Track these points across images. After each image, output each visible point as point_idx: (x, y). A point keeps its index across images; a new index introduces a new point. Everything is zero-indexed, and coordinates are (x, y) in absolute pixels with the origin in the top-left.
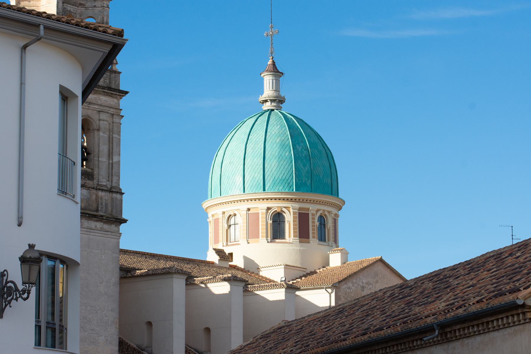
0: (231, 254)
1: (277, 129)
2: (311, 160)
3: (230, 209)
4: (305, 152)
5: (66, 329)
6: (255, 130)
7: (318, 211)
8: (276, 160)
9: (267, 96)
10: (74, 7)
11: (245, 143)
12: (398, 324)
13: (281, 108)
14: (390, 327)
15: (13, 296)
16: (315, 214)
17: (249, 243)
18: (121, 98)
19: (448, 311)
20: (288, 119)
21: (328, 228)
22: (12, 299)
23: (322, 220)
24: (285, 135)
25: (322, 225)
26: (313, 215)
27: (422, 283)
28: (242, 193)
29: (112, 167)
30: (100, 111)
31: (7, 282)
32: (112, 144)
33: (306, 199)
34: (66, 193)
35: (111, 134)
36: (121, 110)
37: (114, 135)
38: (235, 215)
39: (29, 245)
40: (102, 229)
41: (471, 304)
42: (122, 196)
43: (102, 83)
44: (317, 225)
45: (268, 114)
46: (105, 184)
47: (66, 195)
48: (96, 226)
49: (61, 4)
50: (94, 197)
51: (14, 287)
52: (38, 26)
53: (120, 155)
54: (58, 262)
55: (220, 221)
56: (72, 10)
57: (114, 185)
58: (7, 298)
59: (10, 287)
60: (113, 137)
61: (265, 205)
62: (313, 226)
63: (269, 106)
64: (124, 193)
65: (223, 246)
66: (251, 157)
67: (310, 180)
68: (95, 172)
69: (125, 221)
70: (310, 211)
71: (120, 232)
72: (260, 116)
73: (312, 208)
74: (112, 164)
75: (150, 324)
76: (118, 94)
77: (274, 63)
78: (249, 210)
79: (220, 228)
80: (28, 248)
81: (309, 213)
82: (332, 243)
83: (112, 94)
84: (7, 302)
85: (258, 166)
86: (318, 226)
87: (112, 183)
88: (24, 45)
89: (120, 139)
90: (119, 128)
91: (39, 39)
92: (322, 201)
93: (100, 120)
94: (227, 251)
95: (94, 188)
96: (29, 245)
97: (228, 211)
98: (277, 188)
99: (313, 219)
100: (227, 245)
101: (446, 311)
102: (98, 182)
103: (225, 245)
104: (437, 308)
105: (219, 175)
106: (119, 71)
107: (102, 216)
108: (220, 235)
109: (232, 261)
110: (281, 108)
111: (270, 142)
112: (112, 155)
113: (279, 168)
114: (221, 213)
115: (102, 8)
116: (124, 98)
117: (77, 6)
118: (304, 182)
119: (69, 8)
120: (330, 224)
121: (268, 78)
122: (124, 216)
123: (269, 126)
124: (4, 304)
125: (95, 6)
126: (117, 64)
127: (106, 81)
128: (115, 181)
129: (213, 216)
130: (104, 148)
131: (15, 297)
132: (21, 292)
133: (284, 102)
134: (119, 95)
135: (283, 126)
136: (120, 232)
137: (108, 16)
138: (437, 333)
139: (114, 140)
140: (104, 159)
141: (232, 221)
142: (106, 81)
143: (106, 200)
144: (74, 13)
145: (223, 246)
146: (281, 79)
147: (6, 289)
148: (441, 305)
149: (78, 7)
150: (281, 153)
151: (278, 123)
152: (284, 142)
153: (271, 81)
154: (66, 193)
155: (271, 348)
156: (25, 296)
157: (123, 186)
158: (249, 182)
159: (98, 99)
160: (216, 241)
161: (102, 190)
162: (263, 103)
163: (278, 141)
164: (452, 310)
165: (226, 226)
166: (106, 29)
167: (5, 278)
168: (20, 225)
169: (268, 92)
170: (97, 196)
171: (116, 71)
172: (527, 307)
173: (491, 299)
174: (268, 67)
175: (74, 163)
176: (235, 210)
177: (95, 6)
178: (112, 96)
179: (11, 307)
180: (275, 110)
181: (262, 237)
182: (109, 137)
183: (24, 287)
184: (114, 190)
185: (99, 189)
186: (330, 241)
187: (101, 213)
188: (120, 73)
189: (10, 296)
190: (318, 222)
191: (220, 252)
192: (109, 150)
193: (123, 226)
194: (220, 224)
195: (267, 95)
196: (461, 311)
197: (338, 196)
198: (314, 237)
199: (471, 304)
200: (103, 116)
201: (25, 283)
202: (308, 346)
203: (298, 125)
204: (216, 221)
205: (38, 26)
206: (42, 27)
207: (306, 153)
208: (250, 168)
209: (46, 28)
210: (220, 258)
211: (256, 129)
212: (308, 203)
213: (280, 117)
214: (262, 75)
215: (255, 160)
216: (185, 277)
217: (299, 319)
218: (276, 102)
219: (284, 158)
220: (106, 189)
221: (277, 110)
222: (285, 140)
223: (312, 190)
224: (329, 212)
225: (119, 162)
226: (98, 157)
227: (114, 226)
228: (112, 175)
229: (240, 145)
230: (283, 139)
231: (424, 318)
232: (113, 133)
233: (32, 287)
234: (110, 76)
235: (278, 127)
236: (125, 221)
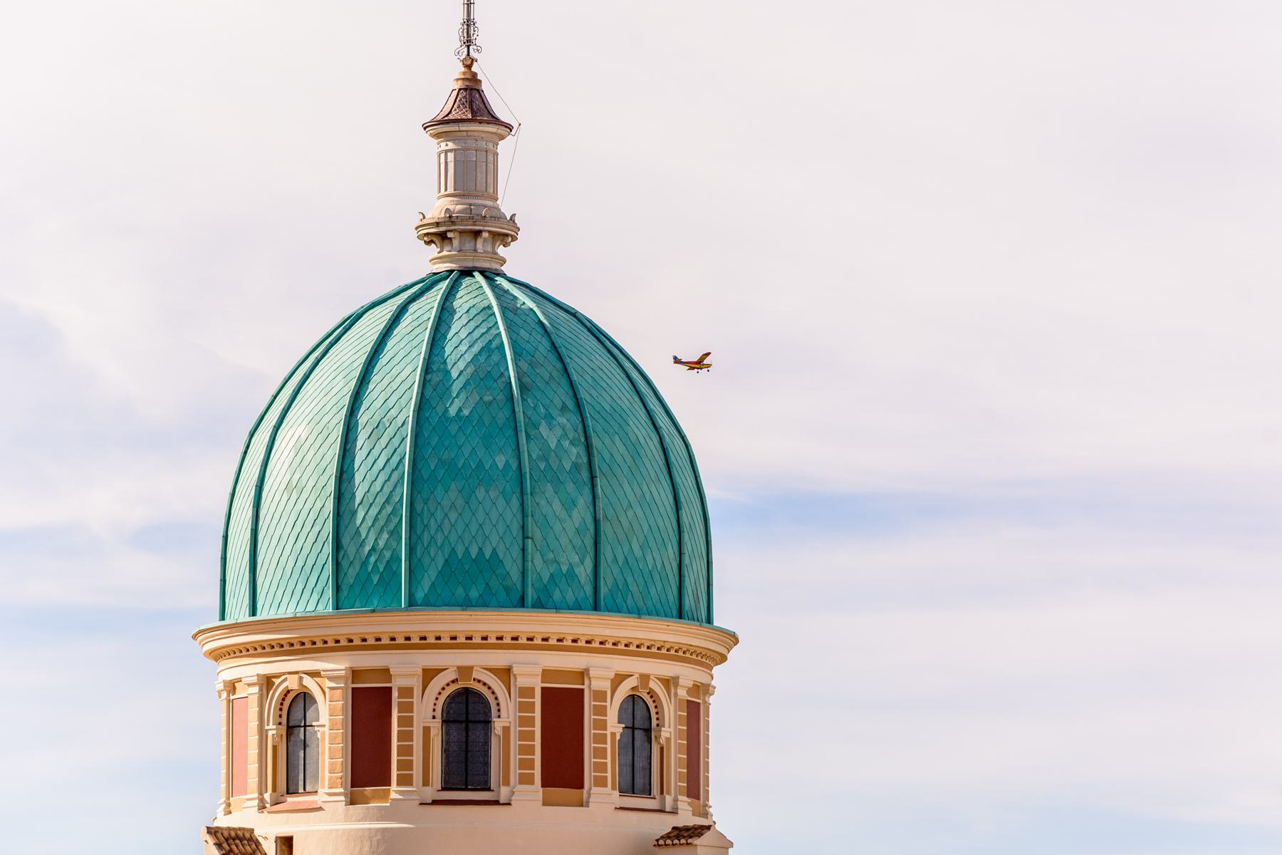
1: (468, 357)
4: (574, 450)
7: (619, 679)
16: (606, 692)
20: (515, 311)
23: (640, 713)
25: (638, 734)
26: (600, 695)
33: (570, 638)
44: (613, 734)
45: (442, 291)
67: (589, 563)
70: (586, 682)
73: (601, 669)
78: (356, 674)
81: (582, 690)
82: (676, 800)
86: (618, 737)
92: (637, 642)
99: (602, 711)
118: (564, 569)
120: (670, 730)
133: (514, 239)
145: (262, 807)
151: (477, 334)
186: (669, 793)
190: (619, 722)
195: (443, 215)
207: (578, 453)
212: (581, 650)
213: (489, 307)
224: (669, 683)
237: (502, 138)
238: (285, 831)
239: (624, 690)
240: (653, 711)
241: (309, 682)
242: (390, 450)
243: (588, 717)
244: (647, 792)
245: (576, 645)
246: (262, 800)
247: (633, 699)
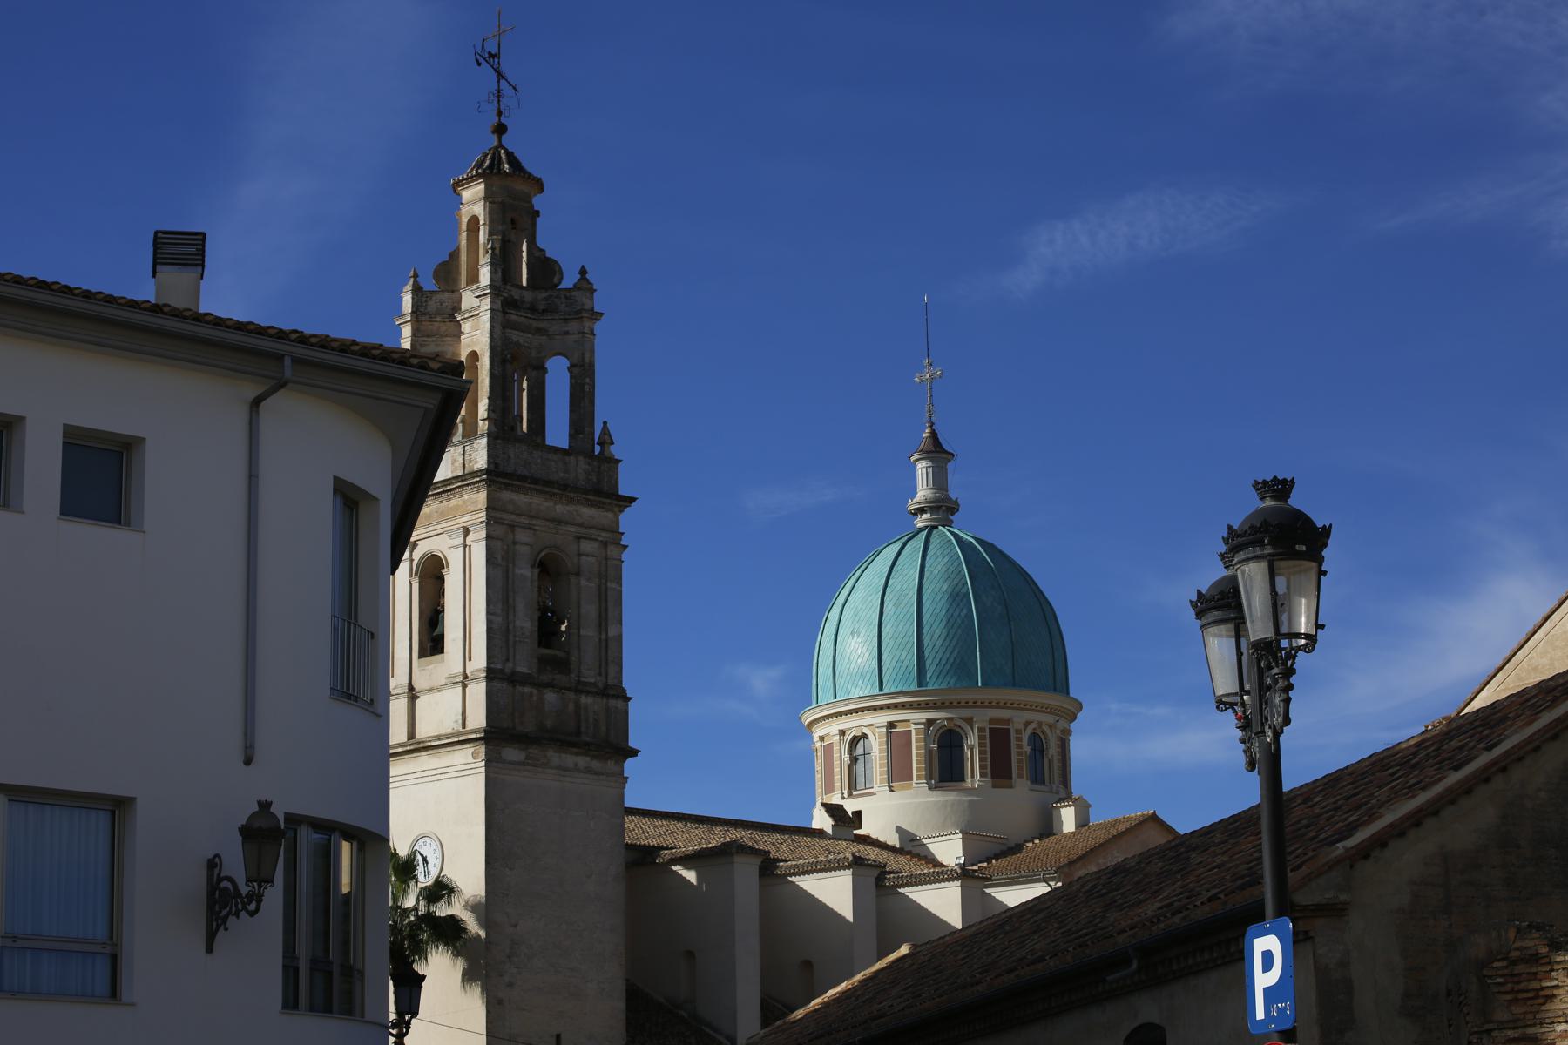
0: (858, 814)
1: (943, 563)
2: (1012, 623)
3: (853, 724)
5: (362, 973)
6: (899, 568)
7: (1027, 724)
8: (942, 626)
9: (922, 499)
10: (525, 335)
11: (880, 593)
12: (1071, 949)
13: (952, 522)
14: (1056, 955)
15: (231, 908)
17: (892, 791)
18: (621, 511)
19: (1159, 920)
21: (1050, 757)
22: (229, 913)
25: (1037, 753)
26: (1018, 731)
27: (1147, 864)
28: (877, 692)
29: (607, 647)
30: (579, 538)
31: (220, 879)
32: (606, 601)
34: (356, 699)
35: (604, 581)
36: (623, 534)
37: (609, 584)
38: (865, 736)
39: (259, 803)
40: (588, 770)
41: (1198, 903)
42: (627, 705)
43: (583, 483)
44: (1026, 752)
46: (593, 680)
47: (356, 701)
48: (576, 765)
49: (498, 329)
50: (571, 707)
51: (231, 888)
52: (281, 358)
53: (621, 624)
54: (337, 833)
55: (836, 748)
56: (521, 341)
57: (610, 682)
58: (220, 912)
59: (226, 889)
60: (606, 589)
61: (922, 716)
62: (1019, 754)
63: (927, 520)
64: (630, 698)
65: (843, 798)
66: (892, 620)
68: (573, 659)
69: (634, 753)
71: (625, 775)
72: (909, 539)
73: (1018, 719)
74: (607, 640)
75: (690, 955)
76: (616, 502)
77: (934, 434)
78: (891, 725)
79: (836, 763)
80: (257, 809)
82: (1058, 787)
83: (603, 503)
84: (219, 921)
85: (906, 639)
87: (606, 677)
88: (254, 400)
89: (620, 593)
90: (619, 569)
91: (281, 385)
93: (580, 555)
94: (850, 806)
95: (569, 689)
96: (259, 803)
97: (850, 729)
98: (948, 679)
99: (1019, 739)
100: (850, 795)
101: (1155, 920)
102: (579, 677)
103: (846, 795)
104: (1143, 915)
105: (831, 658)
106: (616, 457)
107: (587, 744)
108: (837, 777)
109: (860, 827)
110: (952, 522)
111: (930, 590)
112: (606, 625)
113: (948, 640)
114: (837, 732)
115: (581, 335)
116: (626, 510)
117: (529, 333)
119: (516, 336)
120: (1053, 750)
121: (924, 464)
122: (632, 743)
123: (928, 558)
124: (215, 924)
125: (567, 333)
126: (612, 443)
127: (590, 477)
128: (612, 670)
129: (822, 739)
130: (590, 610)
131: (234, 909)
132: (245, 900)
133: (958, 510)
134: (616, 505)
135: (954, 558)
136: (625, 775)
137: (592, 351)
138: (1135, 966)
139: (609, 593)
140: (589, 631)
141: (860, 750)
142: (590, 477)
143: (594, 712)
144: (525, 347)
145: (843, 798)
146: (950, 466)
147: (217, 892)
148: (1151, 908)
149: (533, 334)
150: (951, 611)
152: (956, 590)
153: (930, 470)
154: (356, 699)
155: (864, 1002)
156: (252, 907)
157: (628, 684)
158: (889, 672)
159: (575, 513)
160: (829, 789)
161: (588, 693)
162: (915, 514)
163: (945, 587)
164: (1165, 917)
165: (846, 758)
166: (426, 362)
167: (216, 871)
168: (248, 761)
169: (923, 491)
170: (577, 704)
171: (610, 458)
172: (1297, 908)
173: (1234, 892)
174: (923, 444)
175: (372, 634)
176: (865, 726)
177: (567, 333)
178: (603, 508)
179: (226, 929)
180: (940, 528)
181: (919, 778)
182: (599, 587)
183: (250, 888)
184: (611, 693)
185: (582, 692)
186: (1054, 783)
187: (585, 738)
188: (618, 461)
189: (225, 908)
191: (834, 811)
192: (600, 616)
193: (630, 765)
194: (836, 755)
196: (1177, 919)
197: (1068, 693)
198: (1021, 776)
199: (1198, 903)
200: (587, 546)
201: (251, 881)
202: (920, 996)
203: (985, 555)
204: (828, 749)
205: (281, 358)
206: (287, 361)
208: (892, 643)
209: (297, 361)
210: (835, 820)
211: (902, 565)
212: (1008, 708)
214: (913, 459)
215: (902, 624)
216: (758, 861)
217: (934, 941)
218: (941, 512)
219: (959, 621)
220: (595, 690)
221: (944, 526)
222: (960, 586)
223: (1014, 684)
225: (619, 638)
226: (579, 629)
227: (613, 762)
228: (607, 663)
229: (870, 599)
231: (1115, 934)
232: (606, 581)
233: (266, 888)
234: (599, 467)
235: (946, 560)
236: (634, 753)
237: (949, 461)
238: (856, 809)
239: (1029, 730)
240: (1044, 742)
241: (866, 731)
242: (905, 610)
243: (1013, 743)
244: (1043, 783)
245: (1004, 706)
246: (842, 794)
247: (1034, 735)
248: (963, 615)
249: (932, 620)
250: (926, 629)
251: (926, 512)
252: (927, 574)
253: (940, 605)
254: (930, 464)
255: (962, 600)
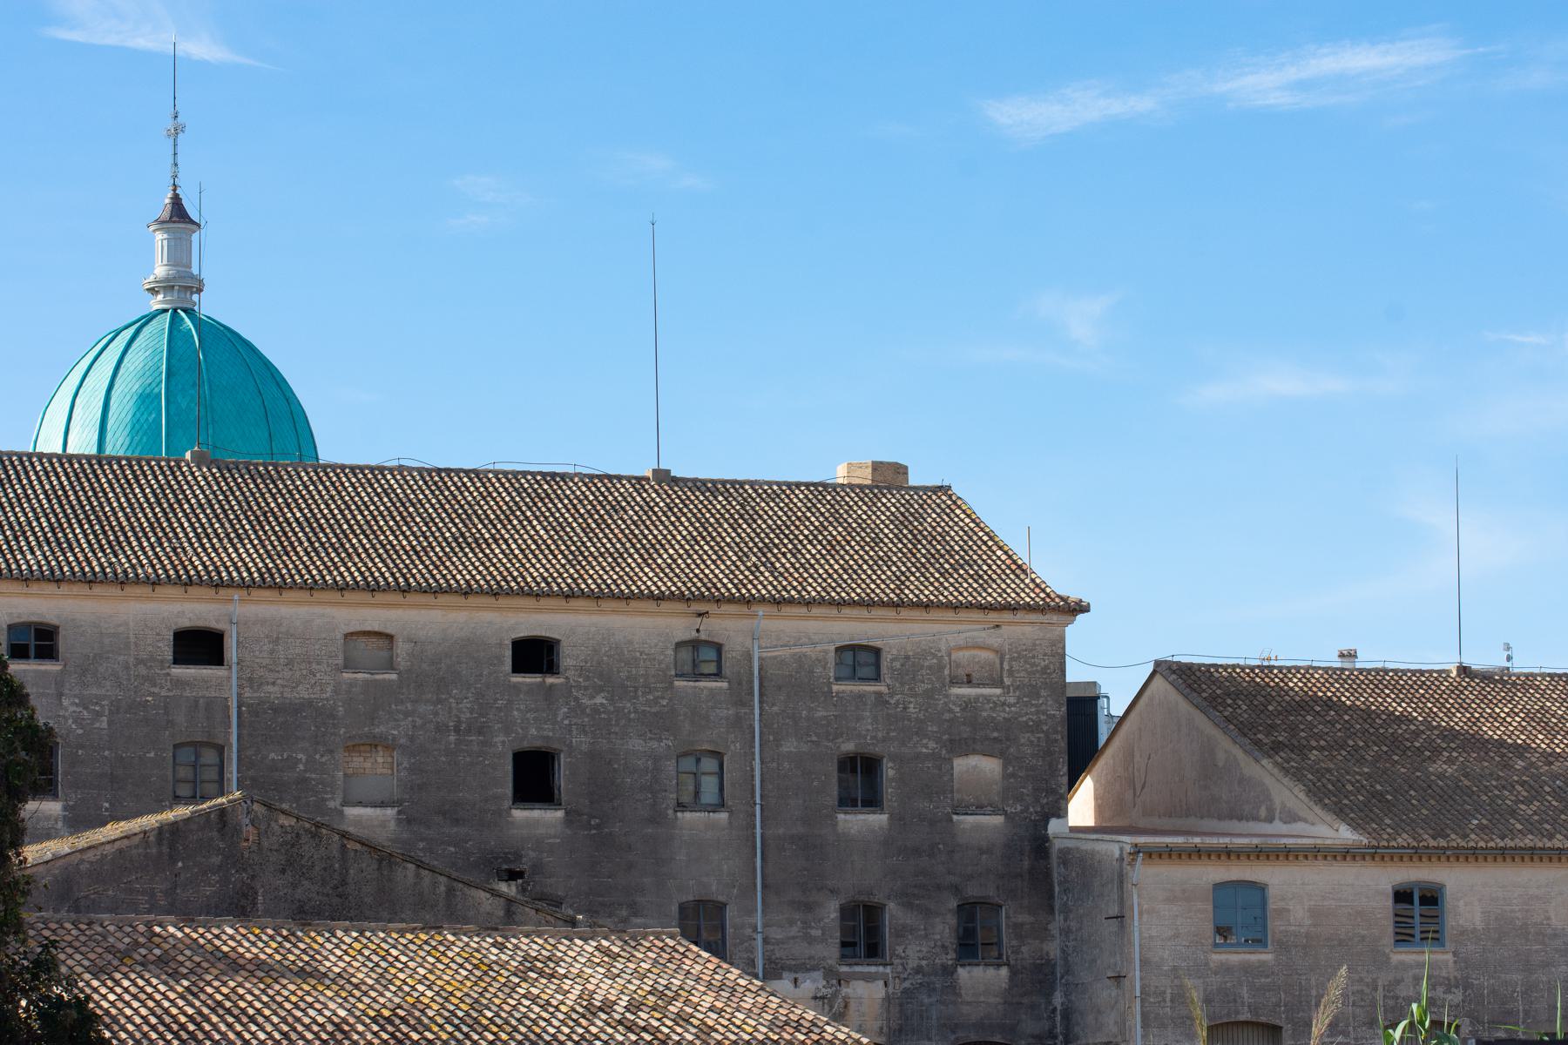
24: (156, 374)
150: (138, 415)
153: (165, 243)
163: (136, 387)
219: (145, 426)
222: (154, 385)
230: (149, 381)
248: (151, 419)
249: (115, 427)
250: (109, 436)
251: (157, 292)
252: (122, 371)
253: (127, 408)
254: (165, 236)
255: (152, 402)
